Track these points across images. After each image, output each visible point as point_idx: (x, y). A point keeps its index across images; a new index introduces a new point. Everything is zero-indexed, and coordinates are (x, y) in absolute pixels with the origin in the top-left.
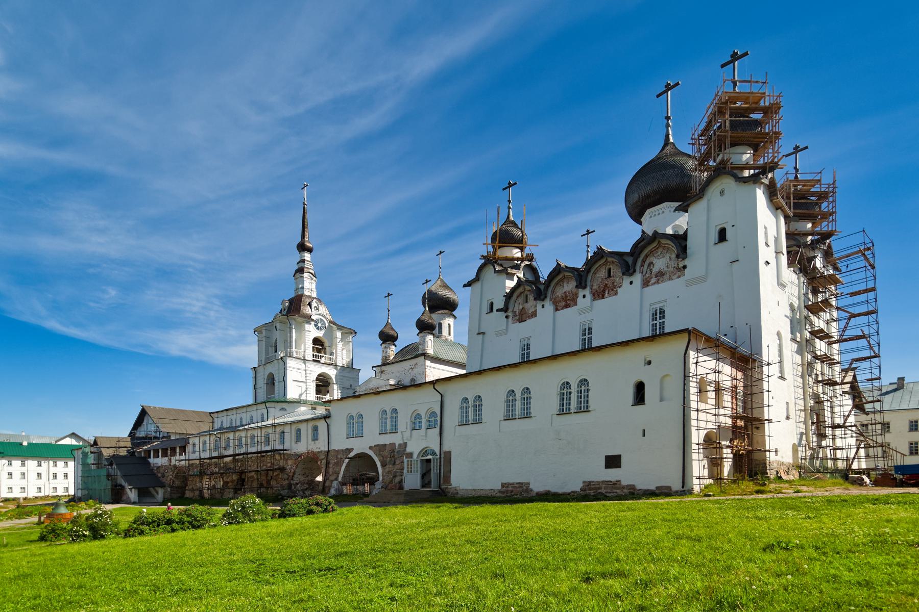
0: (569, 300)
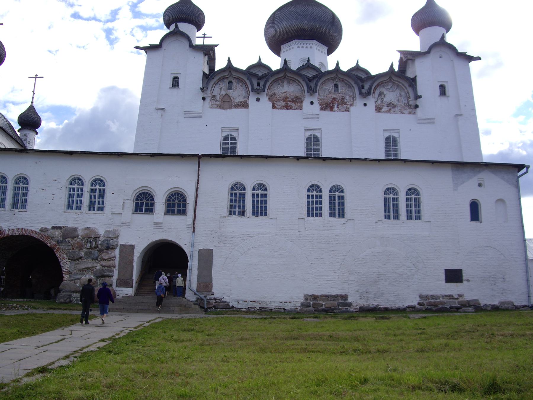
0: (290, 101)
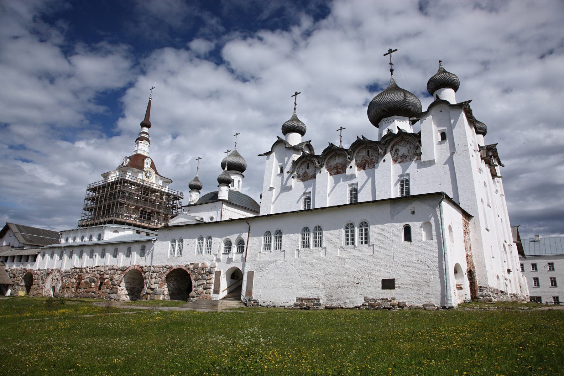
0: (339, 169)
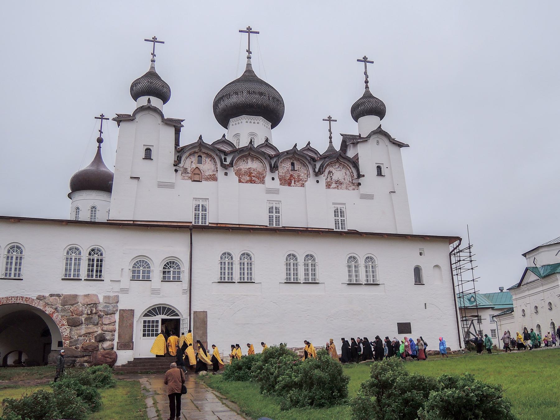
0: (254, 176)
